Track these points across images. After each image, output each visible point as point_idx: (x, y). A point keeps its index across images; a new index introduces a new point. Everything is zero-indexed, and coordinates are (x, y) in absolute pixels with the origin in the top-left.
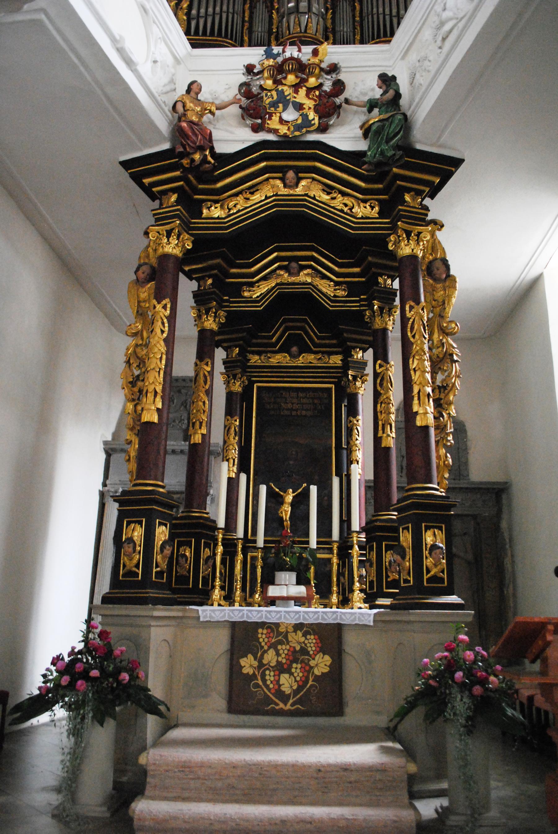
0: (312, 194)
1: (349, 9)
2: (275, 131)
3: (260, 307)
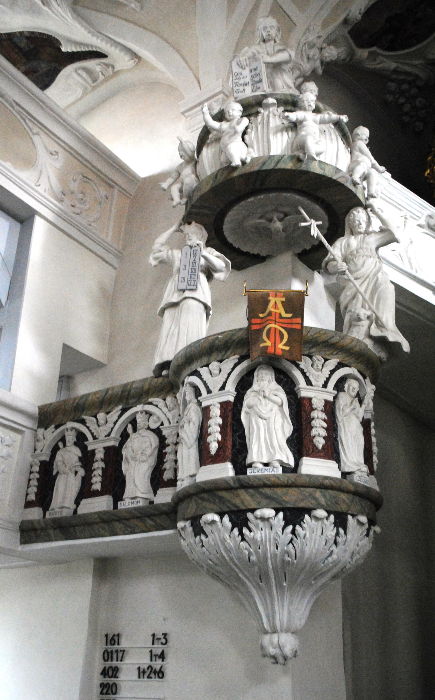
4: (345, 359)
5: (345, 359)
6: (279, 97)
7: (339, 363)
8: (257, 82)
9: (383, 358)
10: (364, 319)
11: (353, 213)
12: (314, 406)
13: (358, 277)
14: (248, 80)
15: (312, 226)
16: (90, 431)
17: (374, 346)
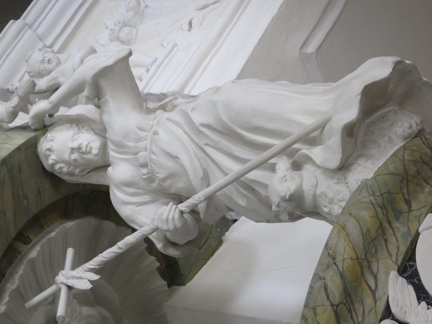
4: (394, 252)
5: (394, 252)
7: (402, 271)
9: (411, 127)
10: (298, 180)
11: (53, 165)
13: (200, 174)
15: (71, 282)
17: (369, 157)
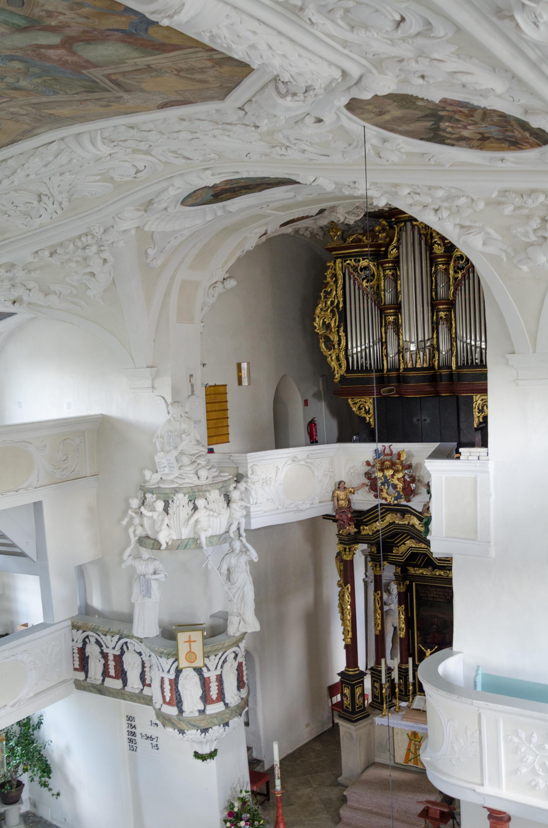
0: (411, 523)
1: (446, 330)
2: (386, 499)
3: (403, 559)
6: (185, 491)
8: (171, 467)
12: (211, 681)
14: (166, 464)
16: (103, 641)
